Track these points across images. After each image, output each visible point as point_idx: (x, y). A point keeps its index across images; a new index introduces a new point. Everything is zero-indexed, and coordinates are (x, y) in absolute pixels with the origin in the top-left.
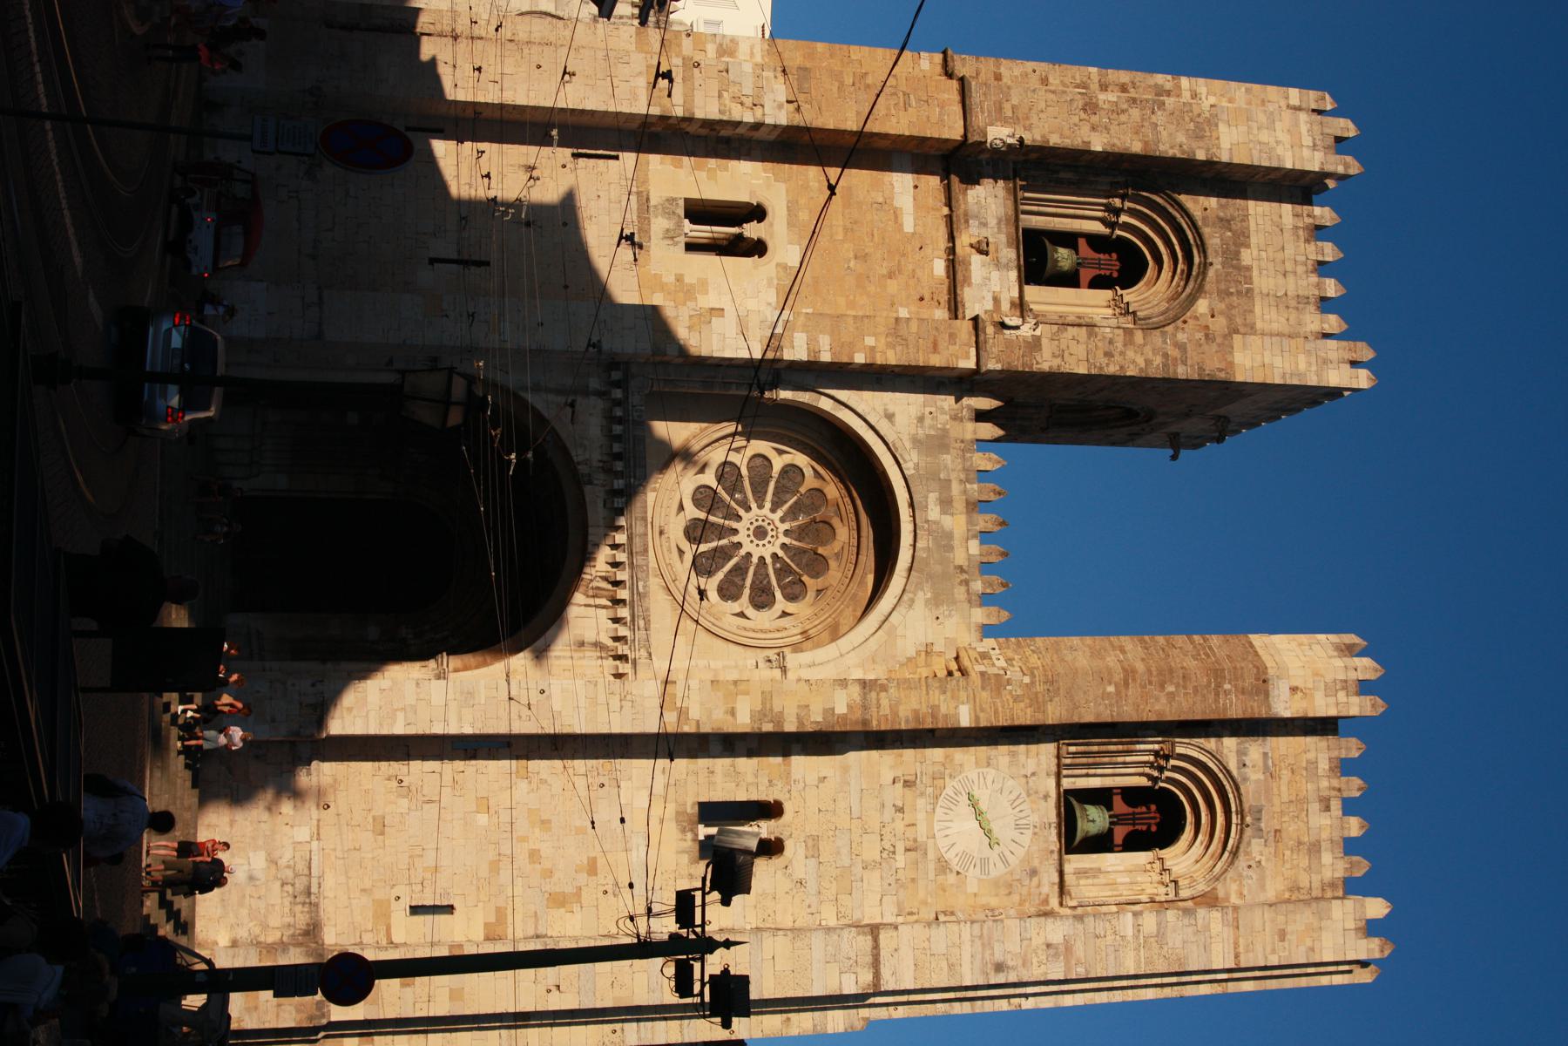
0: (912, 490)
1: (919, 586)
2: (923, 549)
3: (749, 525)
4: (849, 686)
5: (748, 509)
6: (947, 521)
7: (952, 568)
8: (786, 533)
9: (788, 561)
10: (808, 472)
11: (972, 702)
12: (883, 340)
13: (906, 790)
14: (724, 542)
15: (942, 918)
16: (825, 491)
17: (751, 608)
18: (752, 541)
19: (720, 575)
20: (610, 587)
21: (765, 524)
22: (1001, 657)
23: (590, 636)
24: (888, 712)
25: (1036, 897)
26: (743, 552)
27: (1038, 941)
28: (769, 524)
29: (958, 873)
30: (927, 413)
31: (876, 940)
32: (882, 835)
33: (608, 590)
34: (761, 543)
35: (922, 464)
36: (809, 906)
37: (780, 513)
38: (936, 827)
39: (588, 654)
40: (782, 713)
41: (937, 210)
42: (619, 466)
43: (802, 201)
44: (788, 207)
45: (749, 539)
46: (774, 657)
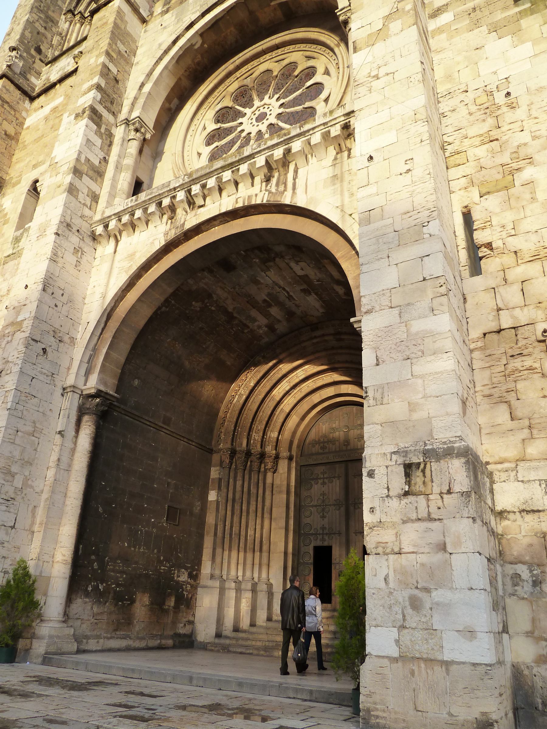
0: (209, 6)
5: (243, 131)
8: (262, 100)
20: (276, 175)
21: (254, 117)
28: (255, 114)
34: (268, 113)
39: (346, 168)
42: (166, 202)
43: (34, 162)
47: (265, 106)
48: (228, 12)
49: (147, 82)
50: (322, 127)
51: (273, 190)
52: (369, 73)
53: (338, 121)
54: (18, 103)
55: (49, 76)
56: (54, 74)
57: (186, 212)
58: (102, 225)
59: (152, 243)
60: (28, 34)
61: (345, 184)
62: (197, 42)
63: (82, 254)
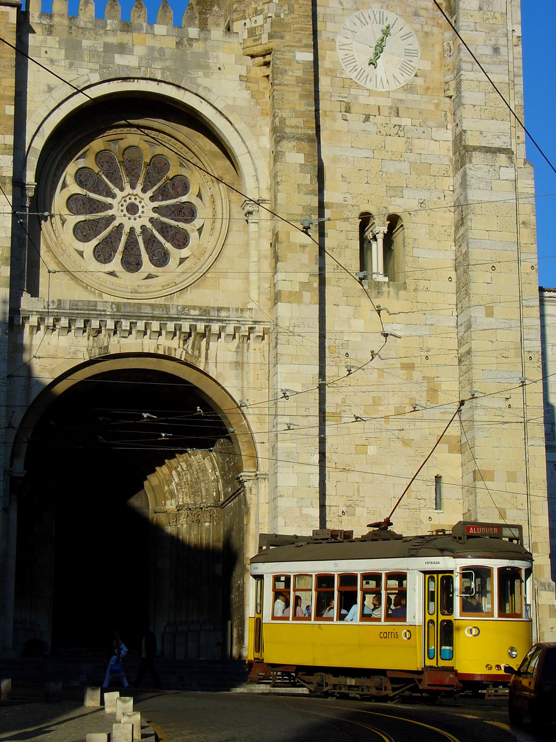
1: (193, 81)
2: (162, 74)
3: (127, 218)
4: (283, 150)
6: (140, 50)
8: (133, 187)
9: (155, 188)
10: (82, 163)
11: (293, 49)
13: (352, 110)
14: (140, 240)
15: (451, 93)
16: (98, 151)
17: (194, 222)
18: (140, 217)
19: (168, 246)
21: (125, 204)
22: (253, 19)
23: (231, 357)
24: (301, 120)
25: (436, 13)
26: (149, 225)
27: (478, 17)
28: (125, 201)
29: (416, 76)
30: (46, 56)
31: (475, 149)
33: (195, 339)
34: (141, 210)
35: (91, 65)
36: (439, 198)
37: (116, 191)
38: (380, 89)
39: (245, 360)
42: (95, 324)
45: (138, 218)
46: (248, 208)
47: (137, 197)
51: (190, 352)
53: (247, 323)
57: (110, 336)
59: (75, 353)
61: (245, 372)
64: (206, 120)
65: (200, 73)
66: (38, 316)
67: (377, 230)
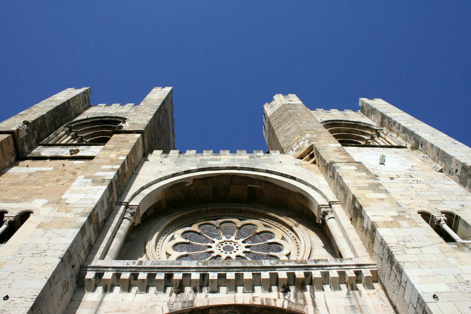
5: (212, 252)
7: (251, 159)
12: (114, 152)
15: (440, 168)
18: (235, 252)
21: (222, 247)
26: (243, 255)
28: (222, 245)
32: (410, 183)
34: (235, 248)
39: (361, 303)
40: (369, 184)
41: (46, 161)
42: (178, 276)
44: (6, 202)
47: (231, 242)
48: (218, 176)
49: (146, 188)
50: (338, 268)
52: (398, 242)
53: (351, 267)
54: (9, 154)
55: (41, 152)
56: (46, 152)
58: (95, 272)
60: (39, 123)
62: (189, 183)
63: (67, 290)
64: (276, 183)
65: (267, 164)
66: (114, 272)
67: (438, 218)
